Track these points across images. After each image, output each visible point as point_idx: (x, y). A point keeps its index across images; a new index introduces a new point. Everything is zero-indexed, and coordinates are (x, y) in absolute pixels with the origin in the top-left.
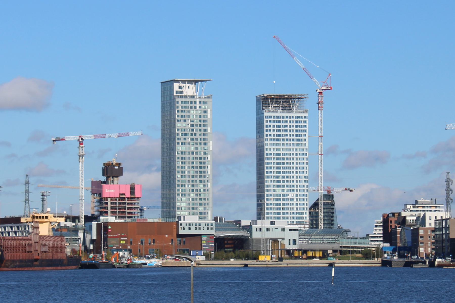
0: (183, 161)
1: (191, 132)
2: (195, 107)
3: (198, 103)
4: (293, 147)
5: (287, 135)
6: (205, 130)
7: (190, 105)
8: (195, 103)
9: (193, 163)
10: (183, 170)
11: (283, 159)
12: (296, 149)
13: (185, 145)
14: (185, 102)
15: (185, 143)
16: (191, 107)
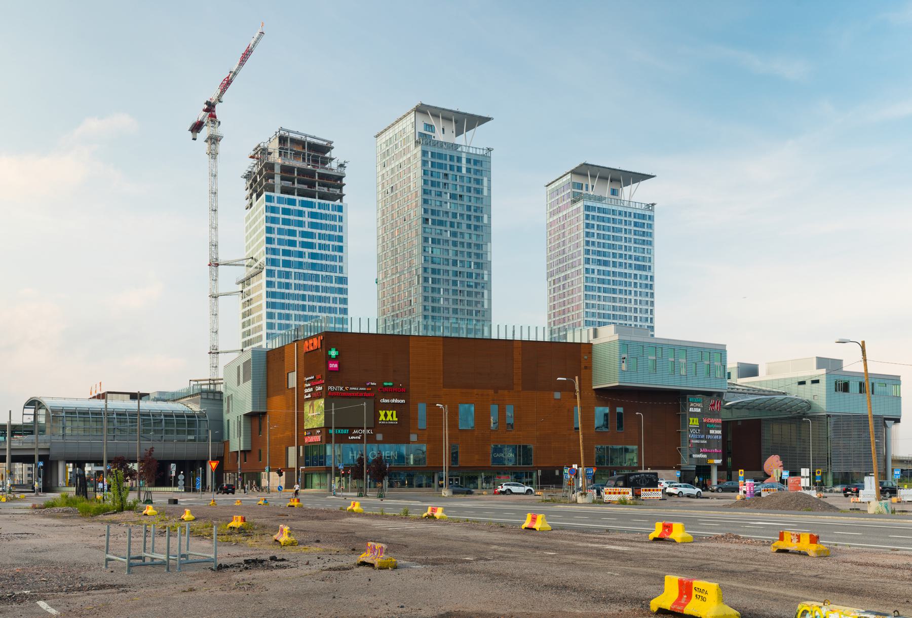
0: (437, 276)
1: (450, 219)
2: (459, 169)
3: (464, 161)
4: (631, 272)
5: (620, 247)
6: (478, 218)
7: (448, 162)
8: (459, 159)
9: (455, 283)
10: (436, 295)
11: (614, 291)
12: (636, 275)
13: (439, 243)
14: (440, 156)
15: (439, 240)
16: (451, 168)
